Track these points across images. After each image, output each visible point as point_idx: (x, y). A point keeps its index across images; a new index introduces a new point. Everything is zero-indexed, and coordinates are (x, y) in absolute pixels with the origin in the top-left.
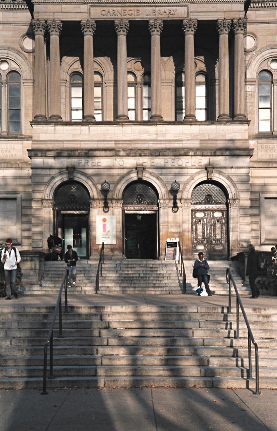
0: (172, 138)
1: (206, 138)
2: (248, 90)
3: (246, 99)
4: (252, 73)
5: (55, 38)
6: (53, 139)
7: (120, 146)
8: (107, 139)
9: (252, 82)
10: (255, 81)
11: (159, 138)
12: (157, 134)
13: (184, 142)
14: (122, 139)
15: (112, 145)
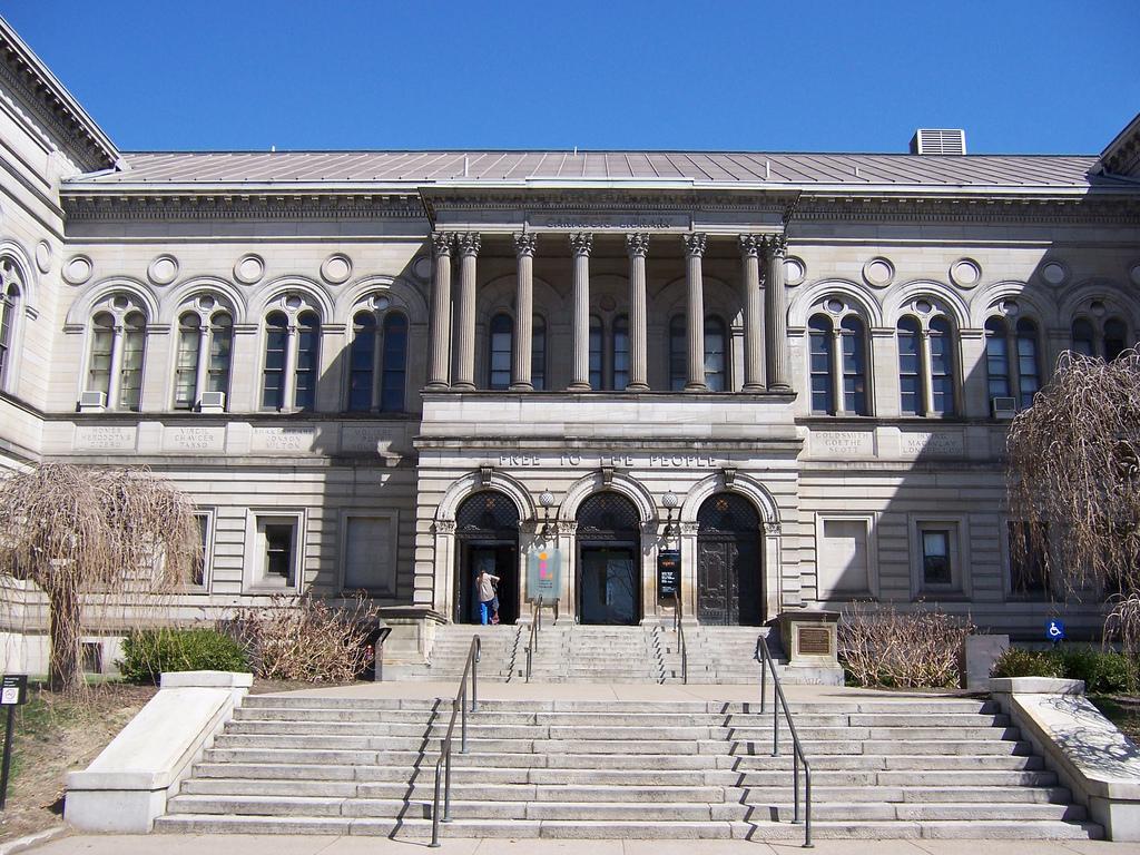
0: (664, 420)
1: (724, 421)
2: (792, 344)
3: (789, 357)
4: (799, 318)
5: (471, 263)
6: (457, 418)
7: (574, 431)
8: (552, 420)
9: (798, 332)
10: (803, 332)
11: (642, 419)
12: (638, 412)
13: (685, 426)
14: (576, 420)
15: (558, 430)
